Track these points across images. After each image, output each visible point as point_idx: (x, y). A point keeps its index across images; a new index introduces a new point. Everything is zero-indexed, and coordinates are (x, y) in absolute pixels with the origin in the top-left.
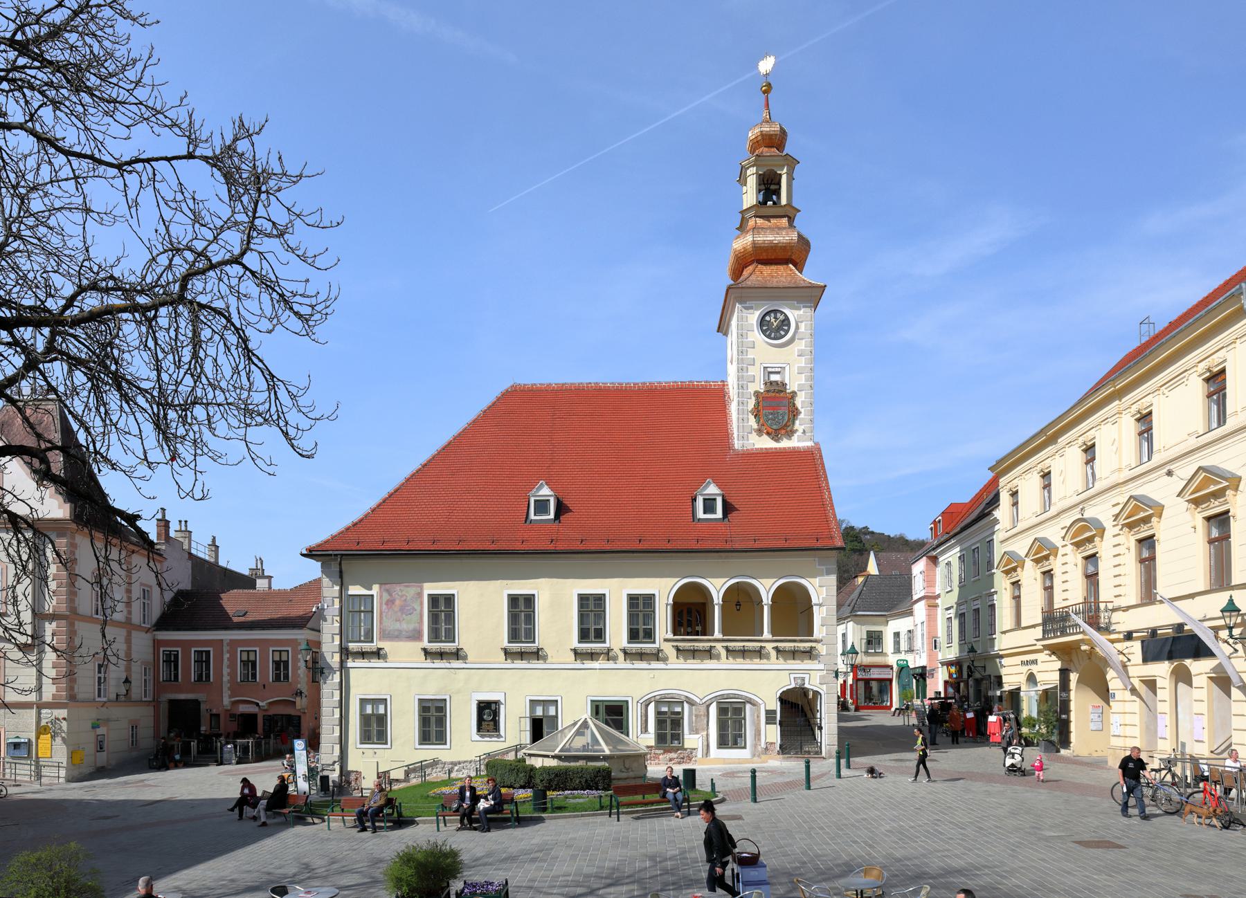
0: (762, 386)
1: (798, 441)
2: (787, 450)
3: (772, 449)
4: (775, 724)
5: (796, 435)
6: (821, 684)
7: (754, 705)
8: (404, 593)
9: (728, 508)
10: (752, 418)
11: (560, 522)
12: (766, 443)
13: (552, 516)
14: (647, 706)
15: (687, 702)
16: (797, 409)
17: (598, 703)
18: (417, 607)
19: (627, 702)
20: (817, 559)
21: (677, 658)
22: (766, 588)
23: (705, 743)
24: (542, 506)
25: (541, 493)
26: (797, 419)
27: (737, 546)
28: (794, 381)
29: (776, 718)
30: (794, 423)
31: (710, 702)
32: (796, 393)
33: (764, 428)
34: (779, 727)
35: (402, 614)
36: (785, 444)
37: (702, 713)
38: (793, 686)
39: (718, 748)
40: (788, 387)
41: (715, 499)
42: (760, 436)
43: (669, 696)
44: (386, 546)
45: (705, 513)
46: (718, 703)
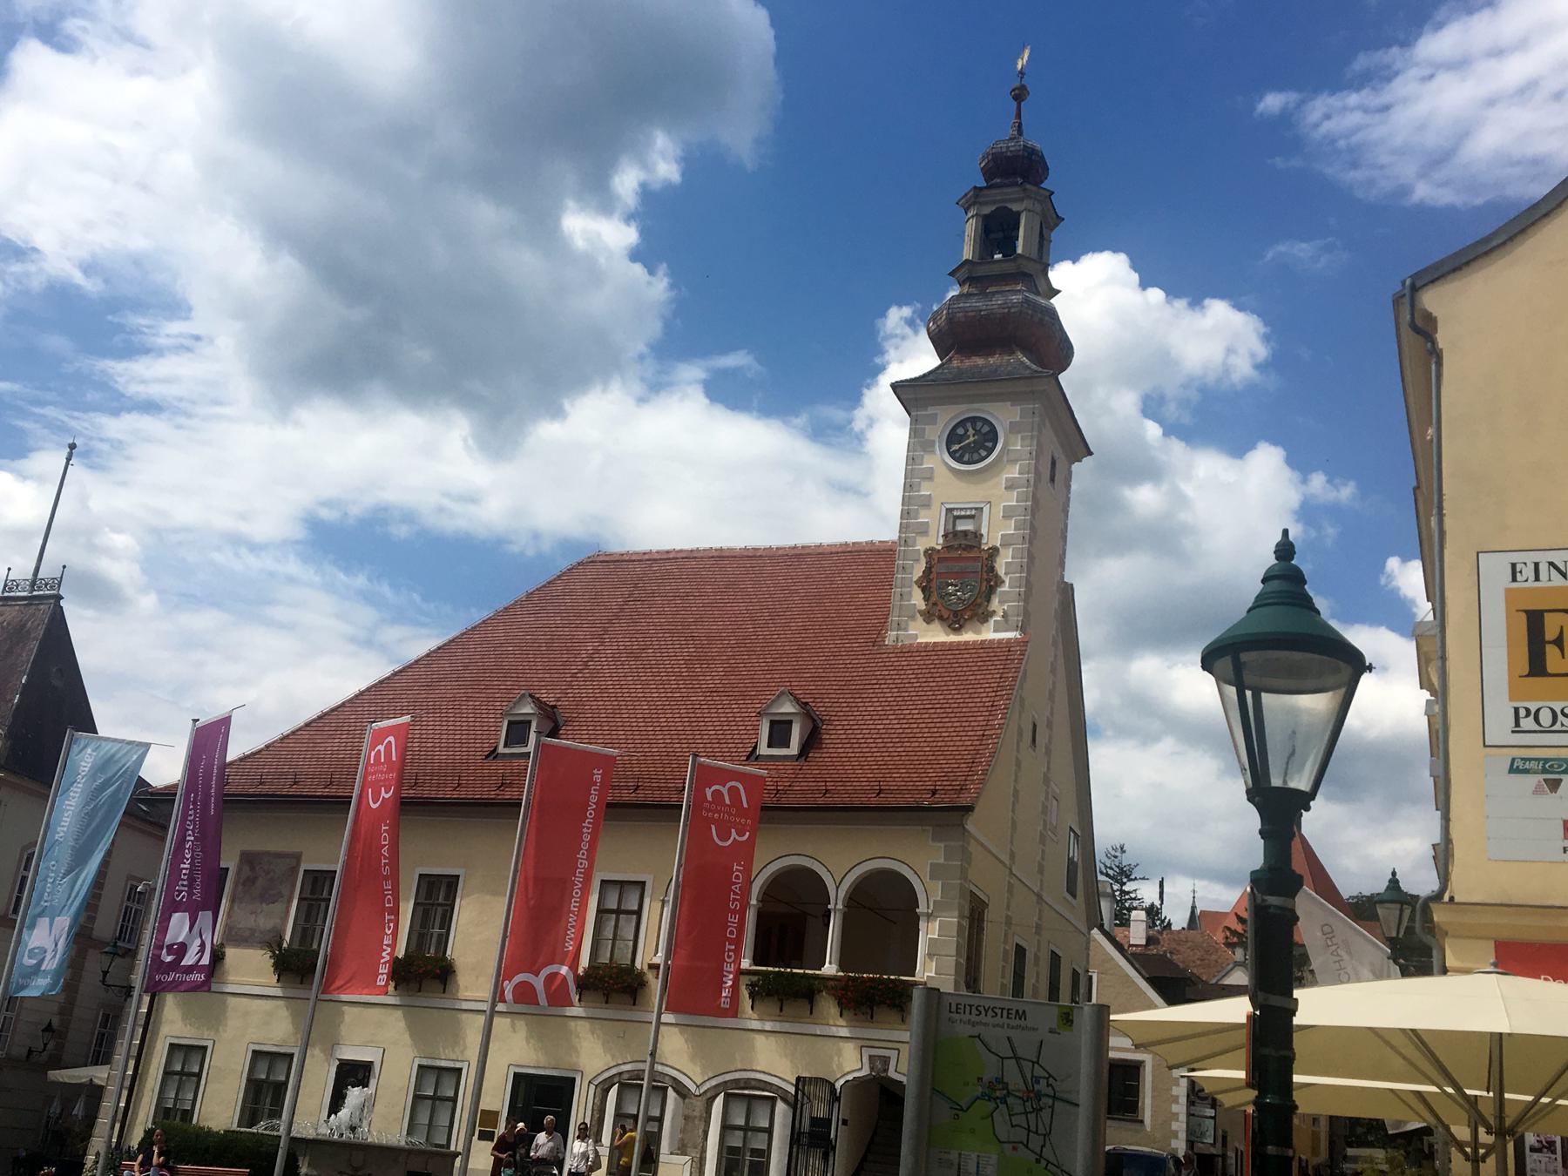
0: (941, 541)
1: (995, 631)
5: (992, 622)
9: (812, 742)
12: (936, 635)
15: (674, 1089)
16: (997, 576)
20: (930, 828)
26: (995, 593)
28: (997, 530)
30: (989, 601)
33: (936, 611)
36: (968, 636)
37: (697, 1113)
38: (865, 1072)
40: (984, 541)
41: (790, 722)
42: (928, 623)
44: (264, 789)
46: (727, 1096)
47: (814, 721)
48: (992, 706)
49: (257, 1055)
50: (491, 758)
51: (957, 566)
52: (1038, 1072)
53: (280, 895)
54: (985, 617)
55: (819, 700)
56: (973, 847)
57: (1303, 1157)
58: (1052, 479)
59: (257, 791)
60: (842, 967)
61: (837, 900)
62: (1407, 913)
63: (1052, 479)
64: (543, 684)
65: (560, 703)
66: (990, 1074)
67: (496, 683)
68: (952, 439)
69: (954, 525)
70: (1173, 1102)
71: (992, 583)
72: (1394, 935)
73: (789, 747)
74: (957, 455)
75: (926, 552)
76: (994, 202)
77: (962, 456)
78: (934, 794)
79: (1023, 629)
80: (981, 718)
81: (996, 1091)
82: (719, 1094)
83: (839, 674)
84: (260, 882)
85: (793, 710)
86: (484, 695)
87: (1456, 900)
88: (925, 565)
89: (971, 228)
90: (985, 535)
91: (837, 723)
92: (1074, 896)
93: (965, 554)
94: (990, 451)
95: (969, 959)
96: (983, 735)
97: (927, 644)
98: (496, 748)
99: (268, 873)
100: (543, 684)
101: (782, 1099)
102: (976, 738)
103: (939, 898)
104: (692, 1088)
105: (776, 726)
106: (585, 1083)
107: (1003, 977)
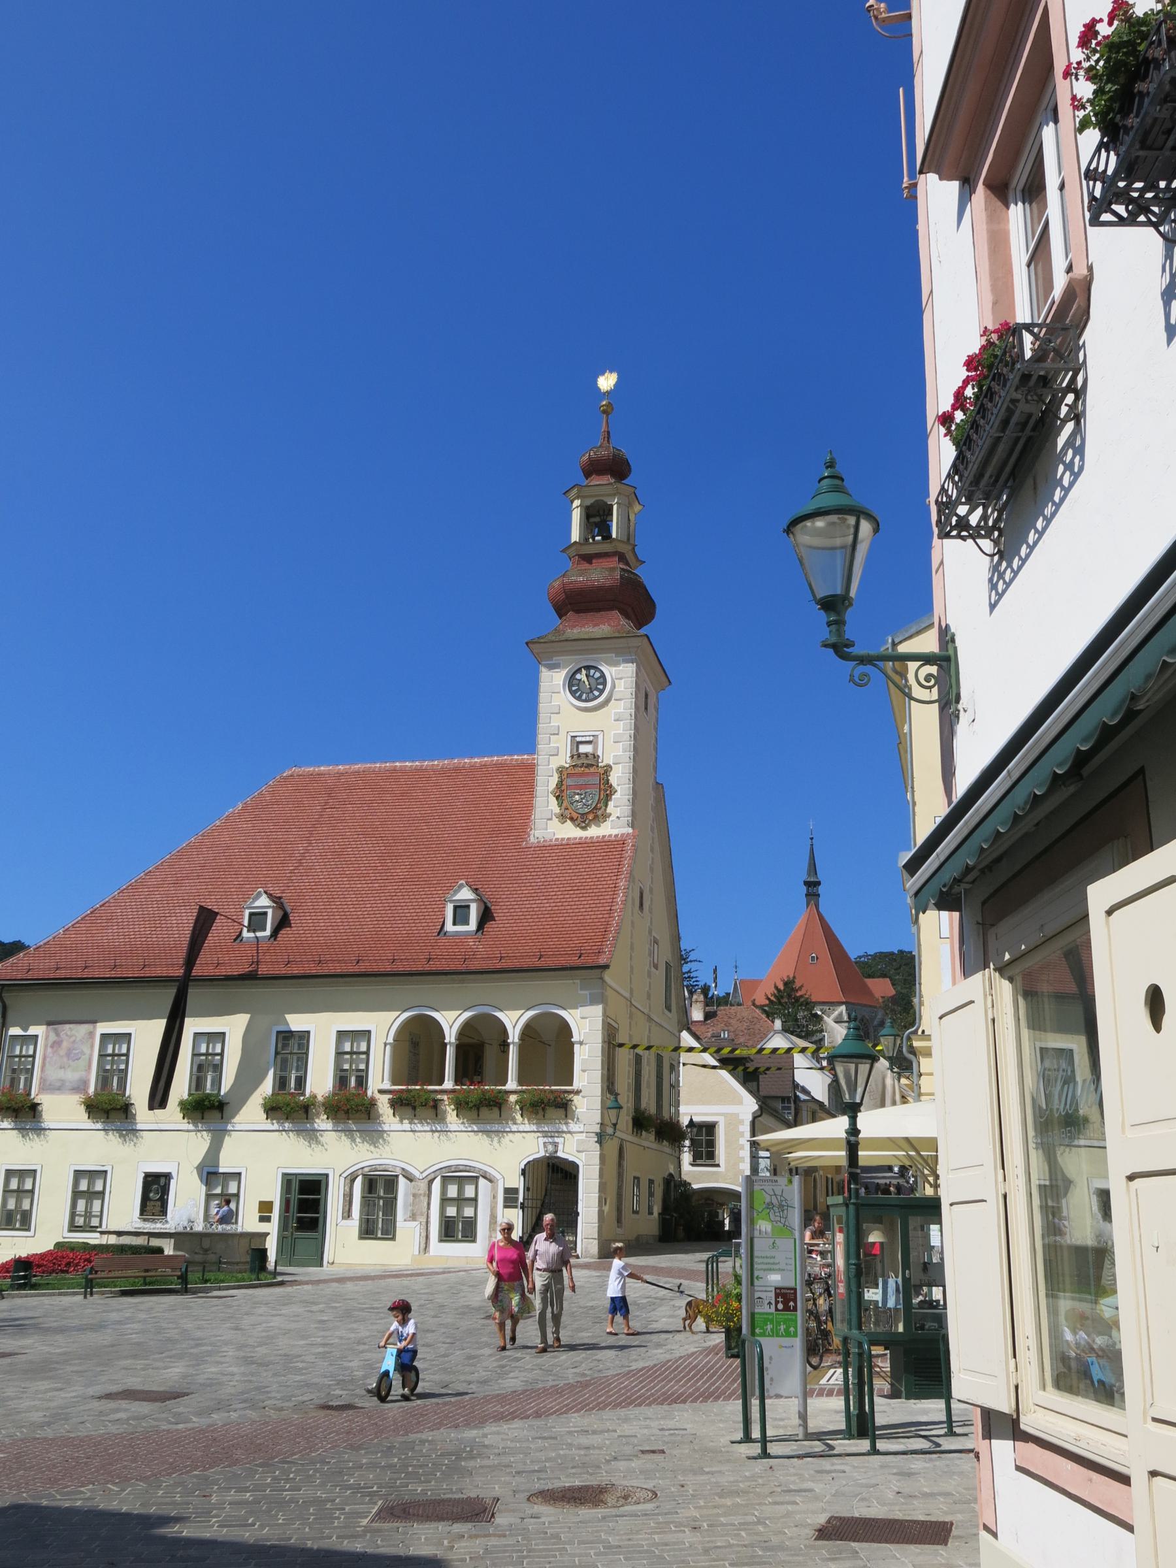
0: (569, 760)
2: (595, 840)
3: (575, 838)
4: (516, 1207)
6: (578, 1151)
7: (490, 1181)
8: (73, 1032)
10: (553, 801)
11: (275, 940)
12: (570, 831)
13: (268, 933)
14: (353, 1181)
15: (404, 1176)
17: (289, 1177)
18: (87, 1050)
19: (327, 1175)
20: (578, 981)
21: (394, 1115)
22: (514, 1021)
23: (424, 1234)
24: (257, 920)
25: (257, 904)
26: (611, 799)
27: (475, 965)
29: (517, 1199)
30: (606, 806)
31: (432, 1176)
32: (611, 767)
33: (567, 813)
34: (521, 1212)
35: (68, 1060)
36: (594, 832)
37: (420, 1192)
38: (542, 1154)
39: (441, 1241)
41: (468, 907)
43: (381, 1168)
44: (58, 975)
45: (454, 924)
46: (443, 1177)
47: (485, 903)
48: (615, 887)
49: (79, 1174)
50: (240, 938)
51: (581, 781)
52: (782, 1199)
53: (83, 1053)
54: (606, 816)
55: (486, 886)
56: (609, 992)
57: (829, 1176)
58: (646, 708)
59: (52, 976)
60: (520, 1083)
61: (514, 1036)
62: (898, 1042)
63: (646, 708)
64: (268, 879)
65: (284, 895)
66: (768, 1200)
67: (230, 880)
68: (572, 683)
69: (577, 750)
70: (740, 1149)
71: (608, 792)
72: (891, 1055)
73: (468, 924)
74: (578, 695)
75: (558, 769)
76: (591, 496)
77: (580, 696)
78: (580, 957)
79: (633, 827)
80: (608, 897)
81: (770, 1206)
82: (435, 1178)
83: (499, 865)
84: (65, 1044)
85: (472, 898)
86: (222, 890)
87: (926, 1033)
88: (557, 780)
89: (576, 516)
90: (600, 755)
91: (502, 904)
92: (670, 1011)
93: (587, 770)
94: (601, 692)
95: (608, 1069)
96: (611, 910)
97: (563, 839)
98: (241, 933)
99: (71, 1037)
100: (268, 879)
101: (485, 1177)
102: (605, 912)
103: (587, 1031)
104: (417, 1174)
105: (458, 909)
106: (337, 1176)
107: (629, 1078)
